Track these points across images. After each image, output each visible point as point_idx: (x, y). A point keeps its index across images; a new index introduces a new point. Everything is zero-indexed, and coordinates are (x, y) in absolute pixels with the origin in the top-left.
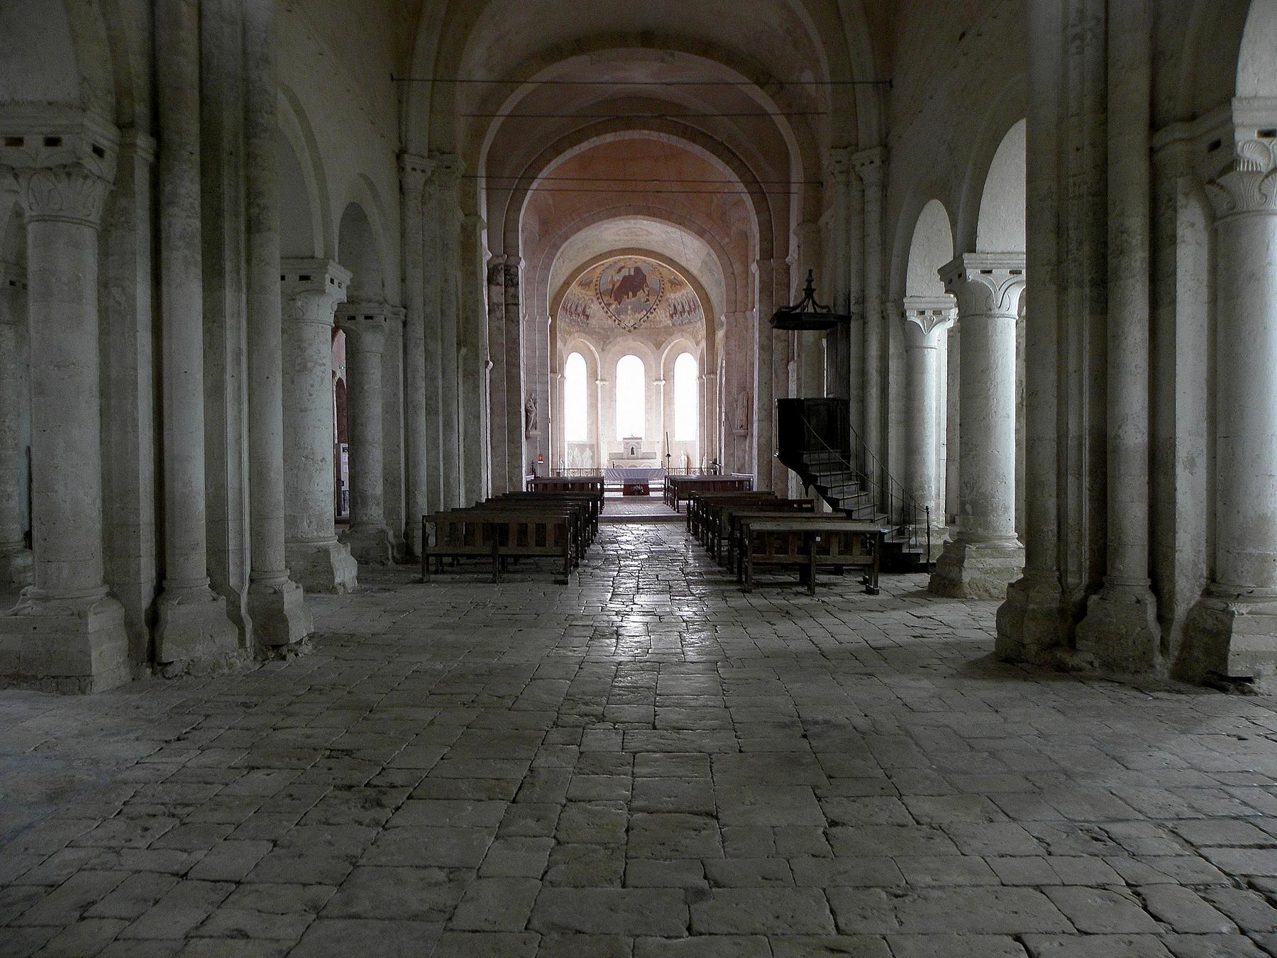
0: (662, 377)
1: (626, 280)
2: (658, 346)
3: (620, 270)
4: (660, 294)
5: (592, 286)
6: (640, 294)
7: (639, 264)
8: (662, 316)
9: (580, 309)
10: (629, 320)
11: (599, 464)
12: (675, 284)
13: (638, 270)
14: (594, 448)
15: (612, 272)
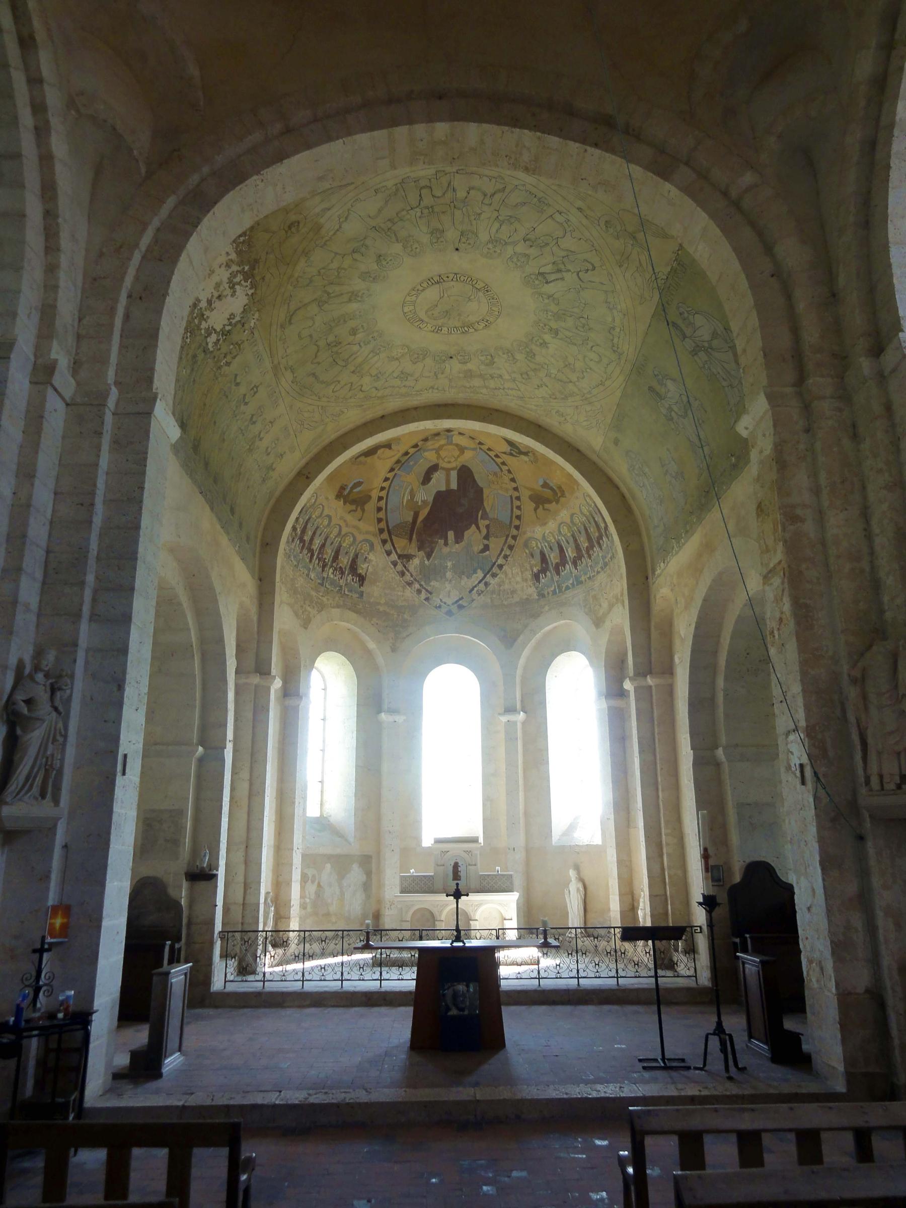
0: (518, 714)
1: (441, 498)
2: (510, 640)
3: (427, 479)
4: (511, 530)
5: (371, 506)
6: (472, 534)
7: (467, 458)
8: (516, 577)
9: (344, 561)
10: (447, 590)
11: (379, 902)
12: (548, 497)
13: (465, 474)
14: (369, 863)
15: (411, 478)
